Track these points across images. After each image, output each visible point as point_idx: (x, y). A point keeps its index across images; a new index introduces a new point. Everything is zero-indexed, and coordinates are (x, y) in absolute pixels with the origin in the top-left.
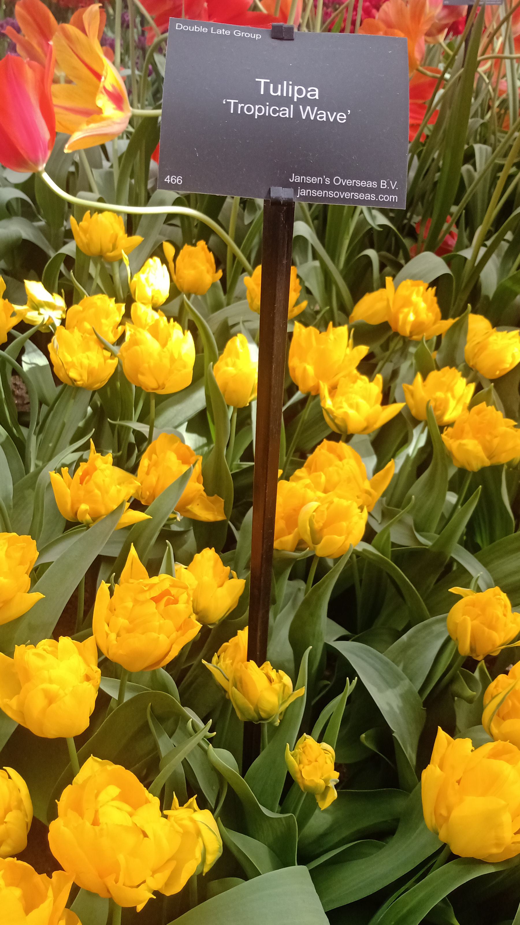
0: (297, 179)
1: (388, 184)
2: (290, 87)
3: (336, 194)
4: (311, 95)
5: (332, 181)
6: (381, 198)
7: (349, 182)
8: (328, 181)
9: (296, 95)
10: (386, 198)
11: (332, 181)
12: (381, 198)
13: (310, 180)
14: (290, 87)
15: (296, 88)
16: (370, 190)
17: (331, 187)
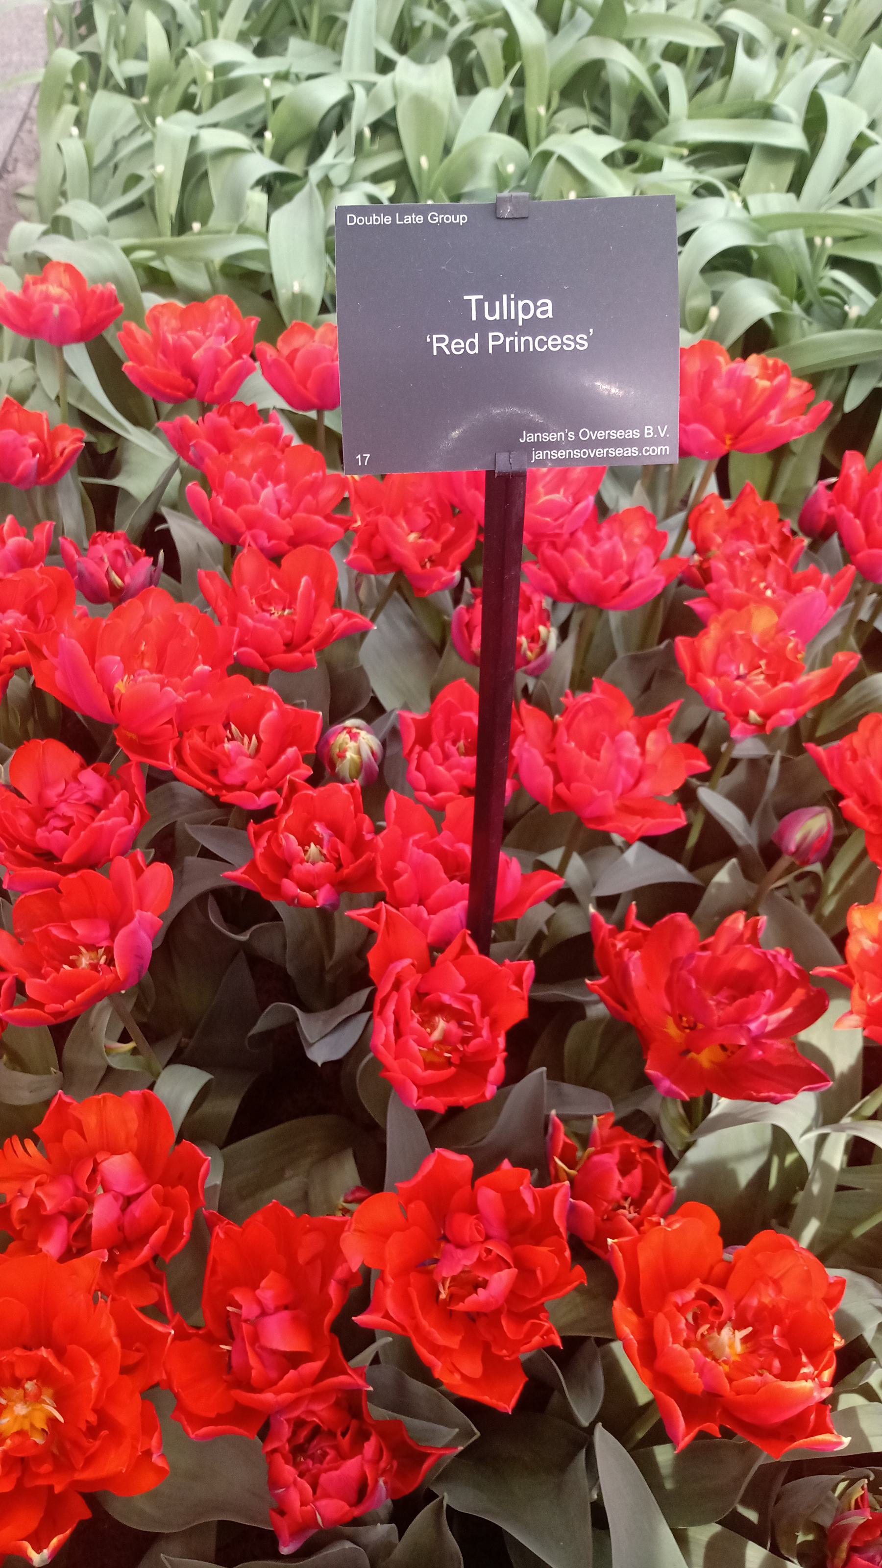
0: (528, 438)
1: (656, 431)
2: (513, 303)
3: (585, 453)
4: (543, 313)
5: (577, 435)
6: (647, 451)
7: (601, 435)
8: (571, 436)
9: (521, 316)
10: (654, 451)
11: (577, 435)
12: (647, 451)
13: (546, 437)
14: (513, 303)
15: (521, 303)
16: (630, 443)
17: (578, 444)
